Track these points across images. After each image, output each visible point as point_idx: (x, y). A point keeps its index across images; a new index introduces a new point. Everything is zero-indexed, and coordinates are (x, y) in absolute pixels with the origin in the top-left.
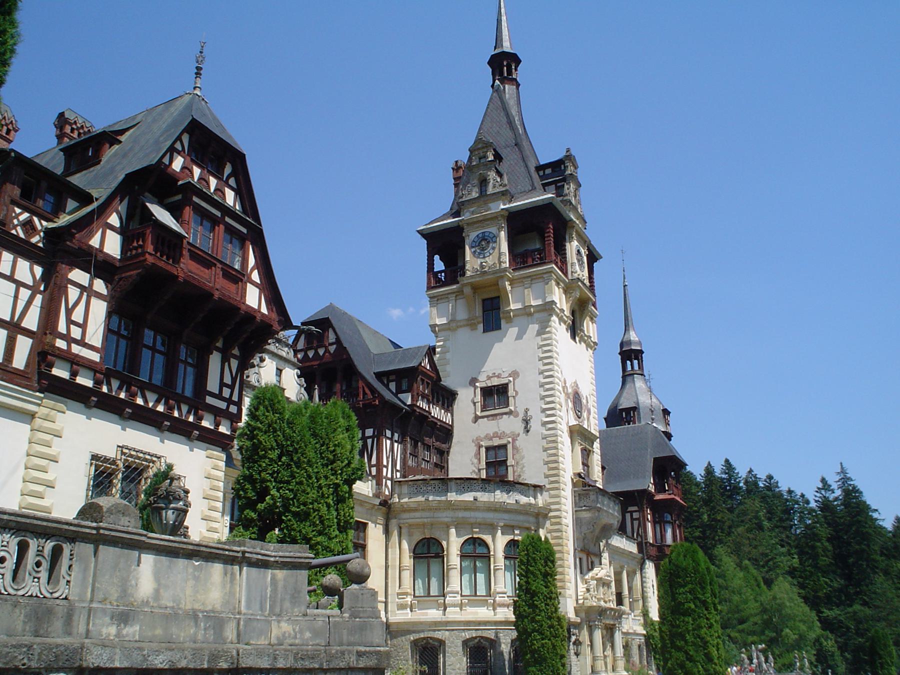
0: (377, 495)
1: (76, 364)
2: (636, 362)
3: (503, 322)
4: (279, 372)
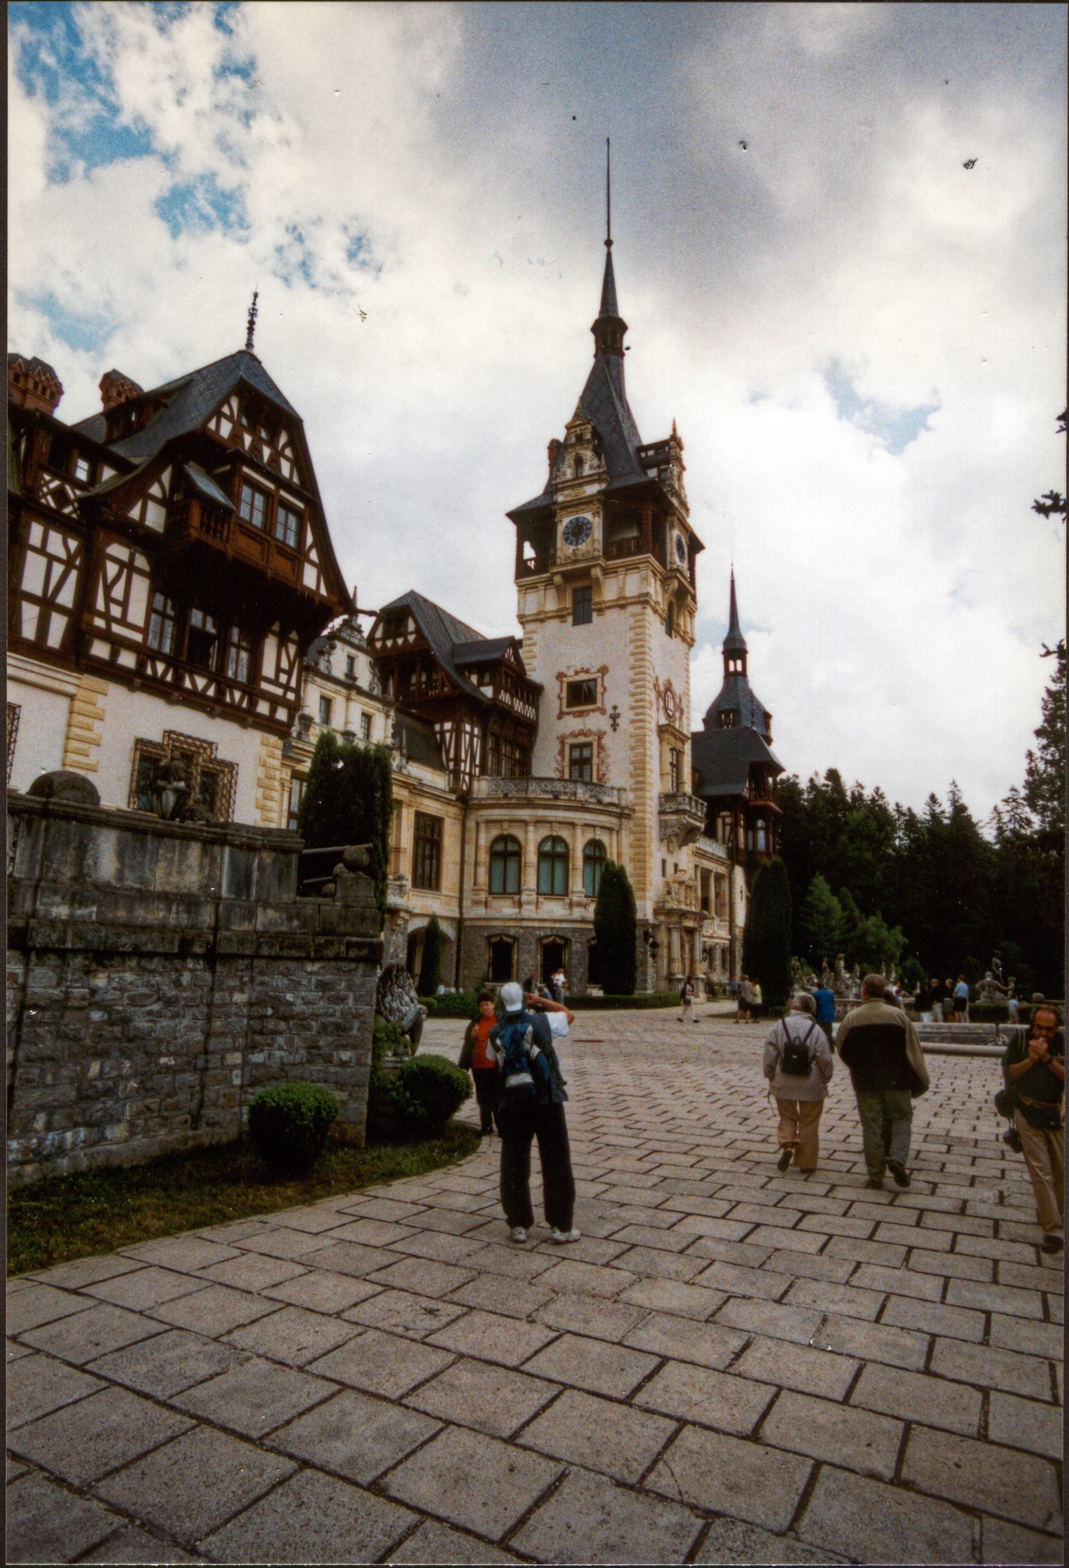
0: (452, 791)
1: (117, 643)
3: (594, 615)
4: (351, 660)
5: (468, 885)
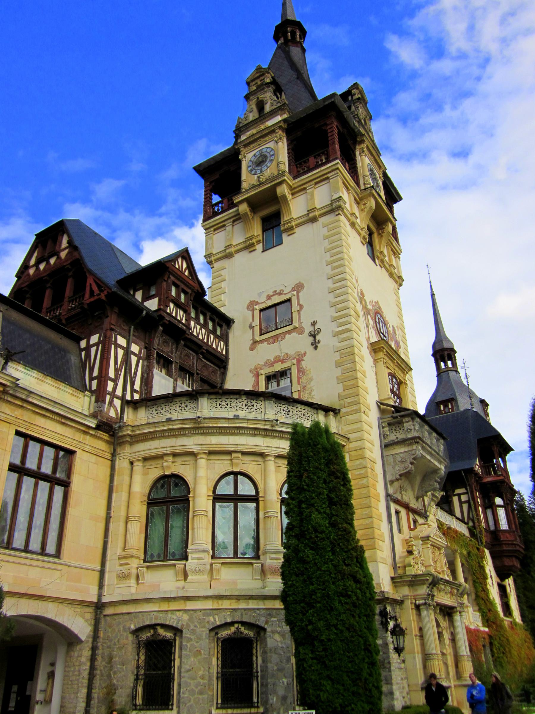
2: (449, 363)
3: (284, 236)
5: (115, 550)
